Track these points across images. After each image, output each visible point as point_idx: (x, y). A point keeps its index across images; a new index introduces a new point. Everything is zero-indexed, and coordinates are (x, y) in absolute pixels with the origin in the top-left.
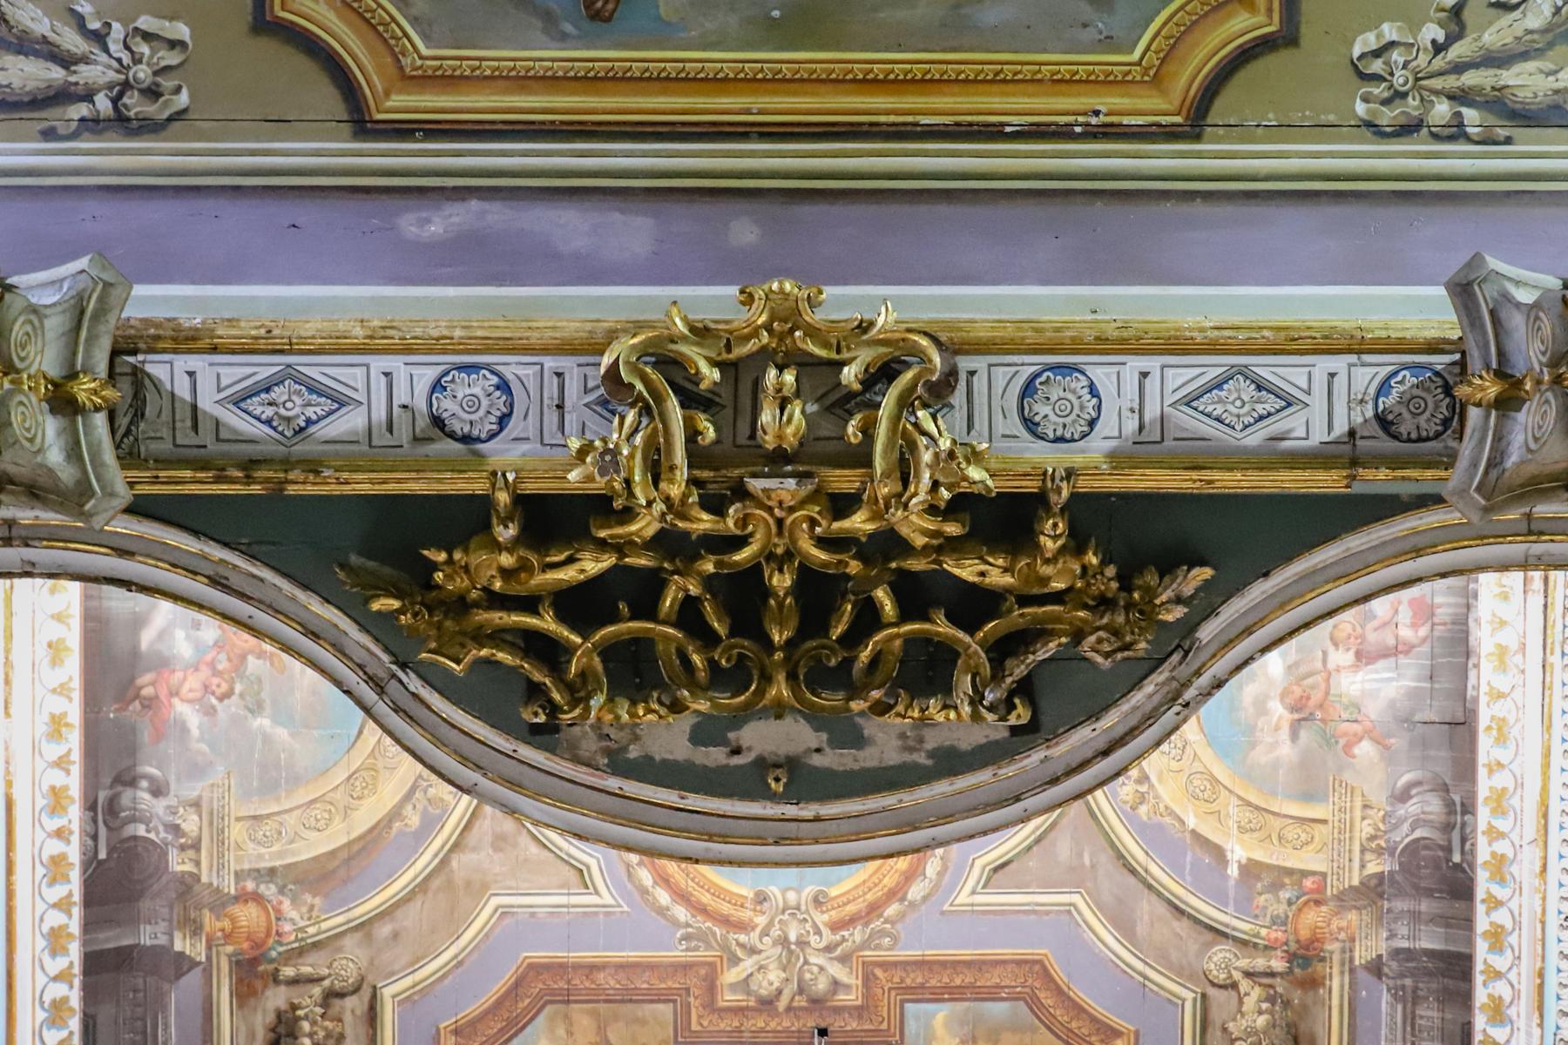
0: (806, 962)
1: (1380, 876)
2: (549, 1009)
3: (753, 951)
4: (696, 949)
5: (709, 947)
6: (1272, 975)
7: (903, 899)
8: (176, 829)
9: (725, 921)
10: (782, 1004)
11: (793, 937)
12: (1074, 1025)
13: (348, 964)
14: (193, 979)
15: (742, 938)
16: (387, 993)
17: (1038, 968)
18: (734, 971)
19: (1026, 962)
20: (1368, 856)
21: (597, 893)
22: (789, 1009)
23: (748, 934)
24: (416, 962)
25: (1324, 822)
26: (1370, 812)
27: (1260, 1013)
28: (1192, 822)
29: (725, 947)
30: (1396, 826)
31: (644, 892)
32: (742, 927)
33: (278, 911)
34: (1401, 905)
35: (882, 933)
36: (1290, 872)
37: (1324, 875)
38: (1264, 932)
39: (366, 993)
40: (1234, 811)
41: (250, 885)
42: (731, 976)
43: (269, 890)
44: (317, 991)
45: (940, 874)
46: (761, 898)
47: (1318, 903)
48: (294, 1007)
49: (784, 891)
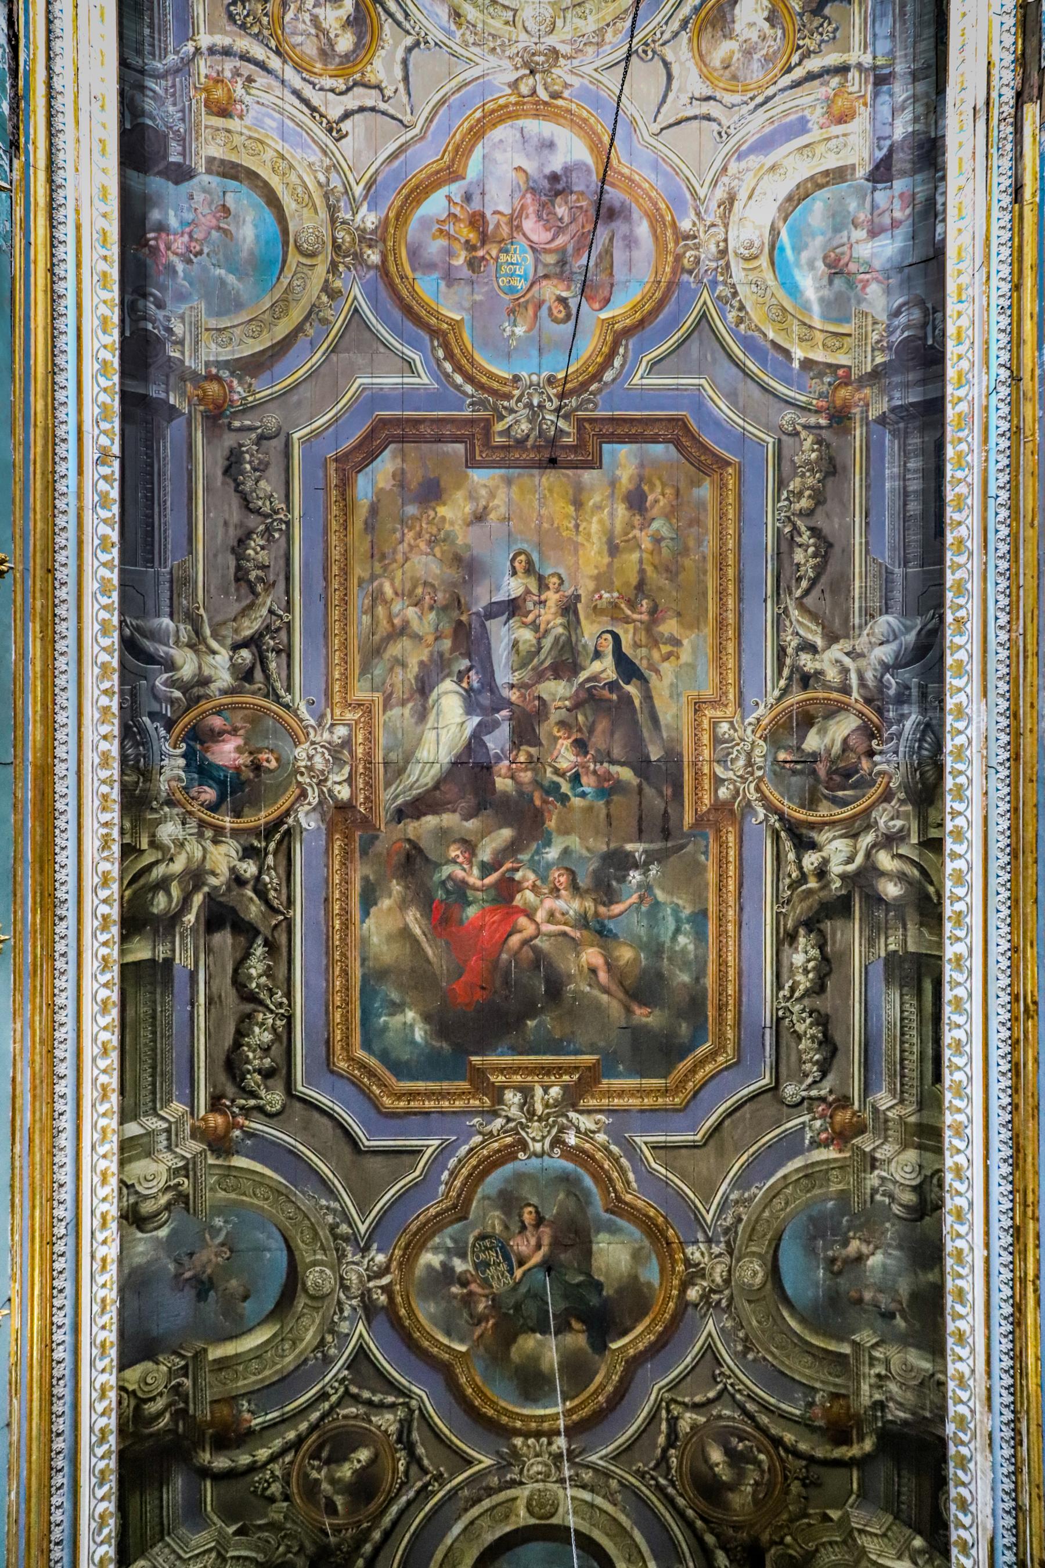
1: (884, 364)
2: (392, 446)
3: (512, 411)
6: (819, 427)
8: (169, 330)
9: (494, 393)
10: (529, 443)
11: (535, 403)
13: (272, 420)
14: (179, 422)
16: (296, 436)
17: (680, 423)
22: (533, 447)
24: (311, 419)
28: (771, 335)
29: (495, 409)
30: (892, 333)
31: (447, 376)
32: (508, 397)
33: (231, 387)
34: (897, 379)
35: (589, 401)
36: (829, 366)
39: (282, 438)
41: (214, 371)
42: (500, 427)
43: (225, 374)
44: (254, 436)
45: (622, 366)
46: (516, 379)
47: (847, 384)
48: (241, 445)
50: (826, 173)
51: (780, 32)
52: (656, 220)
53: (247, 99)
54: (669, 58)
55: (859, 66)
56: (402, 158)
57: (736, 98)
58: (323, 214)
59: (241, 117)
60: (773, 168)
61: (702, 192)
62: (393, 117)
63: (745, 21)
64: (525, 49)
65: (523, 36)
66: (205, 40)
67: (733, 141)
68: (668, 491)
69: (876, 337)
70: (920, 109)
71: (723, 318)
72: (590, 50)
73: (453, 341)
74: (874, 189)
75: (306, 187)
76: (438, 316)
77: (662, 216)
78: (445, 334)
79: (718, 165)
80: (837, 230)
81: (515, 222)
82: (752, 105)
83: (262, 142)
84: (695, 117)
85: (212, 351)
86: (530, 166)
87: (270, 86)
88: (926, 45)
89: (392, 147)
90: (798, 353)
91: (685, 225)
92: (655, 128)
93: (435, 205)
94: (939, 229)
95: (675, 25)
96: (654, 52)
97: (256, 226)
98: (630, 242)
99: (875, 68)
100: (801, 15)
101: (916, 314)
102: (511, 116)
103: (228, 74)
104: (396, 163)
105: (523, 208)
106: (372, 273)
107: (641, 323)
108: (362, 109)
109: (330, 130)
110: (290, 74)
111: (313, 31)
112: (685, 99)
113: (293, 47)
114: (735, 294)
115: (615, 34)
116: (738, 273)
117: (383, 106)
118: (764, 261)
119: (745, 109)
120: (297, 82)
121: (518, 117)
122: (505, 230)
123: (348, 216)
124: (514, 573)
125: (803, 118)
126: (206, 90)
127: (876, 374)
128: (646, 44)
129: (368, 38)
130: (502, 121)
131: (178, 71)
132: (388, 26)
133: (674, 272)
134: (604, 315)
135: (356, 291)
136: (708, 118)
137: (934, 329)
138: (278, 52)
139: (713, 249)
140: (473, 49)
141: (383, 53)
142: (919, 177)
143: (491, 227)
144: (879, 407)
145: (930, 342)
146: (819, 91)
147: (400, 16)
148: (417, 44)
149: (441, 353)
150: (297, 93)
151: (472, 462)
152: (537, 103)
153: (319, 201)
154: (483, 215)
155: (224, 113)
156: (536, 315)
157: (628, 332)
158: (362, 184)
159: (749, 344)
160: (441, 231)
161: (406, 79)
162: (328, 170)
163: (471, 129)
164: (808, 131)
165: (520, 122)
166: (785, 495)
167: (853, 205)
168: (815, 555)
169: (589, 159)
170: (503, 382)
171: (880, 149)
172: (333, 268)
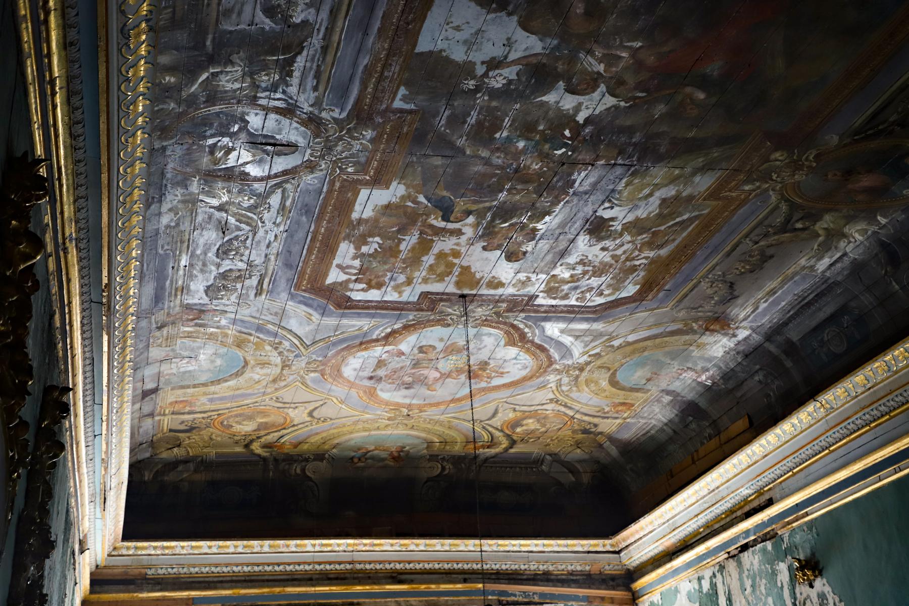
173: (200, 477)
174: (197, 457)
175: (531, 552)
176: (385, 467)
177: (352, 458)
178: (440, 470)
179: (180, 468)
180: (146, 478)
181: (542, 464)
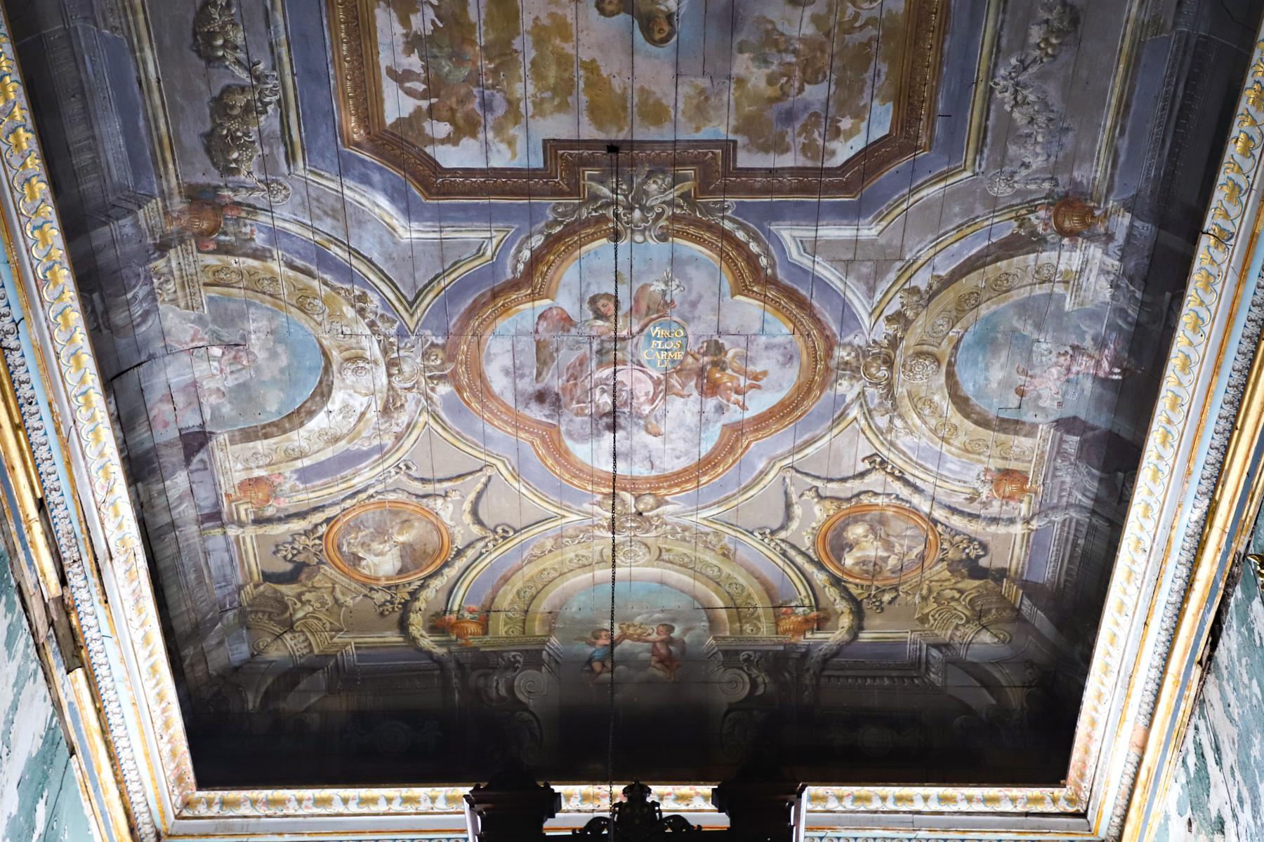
0: (626, 196)
3: (671, 204)
4: (715, 203)
5: (706, 205)
7: (548, 236)
12: (398, 152)
15: (678, 211)
18: (686, 189)
19: (444, 194)
20: (166, 270)
21: (794, 238)
23: (674, 214)
25: (206, 284)
26: (171, 297)
27: (236, 161)
29: (693, 206)
30: (149, 294)
31: (756, 239)
37: (199, 251)
38: (244, 214)
40: (284, 292)
42: (688, 186)
45: (519, 251)
46: (663, 238)
49: (645, 240)
50: (266, 436)
51: (345, 549)
52: (484, 391)
53: (978, 485)
54: (476, 530)
55: (241, 524)
56: (799, 442)
57: (392, 497)
58: (900, 391)
59: (987, 470)
60: (336, 439)
61: (425, 417)
62: (807, 474)
63: (389, 556)
64: (647, 532)
65: (649, 542)
66: (1018, 529)
67: (390, 461)
68: (445, 114)
69: (171, 286)
70: (160, 502)
71: (385, 300)
72: (571, 532)
73: (747, 273)
74: (203, 425)
75: (919, 415)
76: (765, 299)
77: (474, 395)
78: (757, 281)
79: (408, 443)
80: (243, 387)
81: (663, 388)
82: (371, 491)
83: (967, 451)
84: (440, 481)
85: (1070, 259)
86: (641, 437)
87: (949, 495)
88: (166, 552)
89: (810, 451)
90: (276, 266)
91: (444, 389)
92: (489, 472)
93: (760, 403)
94: (113, 407)
95: (471, 553)
96: (495, 531)
97: (986, 379)
98: (515, 372)
99: (223, 526)
100: (320, 562)
101: (119, 318)
102: (666, 478)
103: (996, 504)
104: (806, 437)
105: (653, 401)
106: (847, 340)
107: (495, 295)
108: (844, 480)
109: (883, 462)
110: (925, 507)
111: (892, 539)
112: (455, 496)
113: (917, 526)
114: (372, 325)
115: (543, 545)
116: (373, 348)
117: (819, 483)
118: (336, 355)
119: (380, 487)
120: (916, 500)
121: (657, 478)
122: (675, 381)
123: (870, 391)
124: (669, 17)
125: (305, 482)
126: (1023, 491)
127: (163, 248)
128: (504, 538)
129: (829, 535)
130: (678, 474)
131: (1054, 508)
132: (806, 543)
133: (457, 346)
134: (543, 304)
135: (866, 322)
136: (423, 481)
137: (93, 311)
138: (936, 522)
139: (406, 368)
140: (707, 530)
141: (814, 525)
142: (148, 445)
143: (693, 383)
144: (149, 214)
145: (96, 296)
146: (285, 504)
147: (792, 553)
148: (773, 533)
149: (763, 261)
150: (916, 489)
151: (729, 148)
152: (635, 489)
153: (906, 405)
154: (702, 393)
155: (1006, 473)
156: (637, 301)
157: (514, 285)
158: (850, 417)
159: (347, 273)
160: (756, 378)
161: (788, 506)
162: (890, 430)
163: (715, 466)
164: (296, 471)
165: (654, 473)
166: (270, 109)
167: (227, 409)
168: (212, 36)
169: (569, 443)
170: (678, 234)
171: (202, 461)
172: (894, 343)
173: (340, 704)
174: (326, 656)
175: (919, 813)
176: (651, 681)
177: (590, 661)
178: (748, 687)
179: (301, 686)
180: (250, 706)
181: (928, 669)
